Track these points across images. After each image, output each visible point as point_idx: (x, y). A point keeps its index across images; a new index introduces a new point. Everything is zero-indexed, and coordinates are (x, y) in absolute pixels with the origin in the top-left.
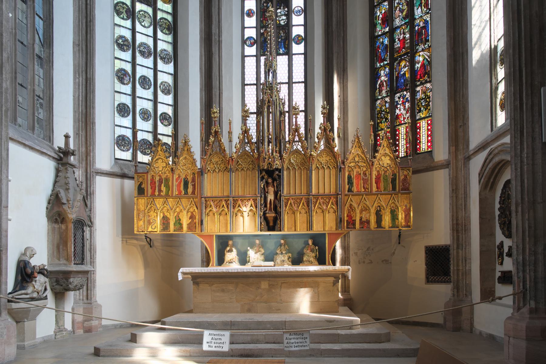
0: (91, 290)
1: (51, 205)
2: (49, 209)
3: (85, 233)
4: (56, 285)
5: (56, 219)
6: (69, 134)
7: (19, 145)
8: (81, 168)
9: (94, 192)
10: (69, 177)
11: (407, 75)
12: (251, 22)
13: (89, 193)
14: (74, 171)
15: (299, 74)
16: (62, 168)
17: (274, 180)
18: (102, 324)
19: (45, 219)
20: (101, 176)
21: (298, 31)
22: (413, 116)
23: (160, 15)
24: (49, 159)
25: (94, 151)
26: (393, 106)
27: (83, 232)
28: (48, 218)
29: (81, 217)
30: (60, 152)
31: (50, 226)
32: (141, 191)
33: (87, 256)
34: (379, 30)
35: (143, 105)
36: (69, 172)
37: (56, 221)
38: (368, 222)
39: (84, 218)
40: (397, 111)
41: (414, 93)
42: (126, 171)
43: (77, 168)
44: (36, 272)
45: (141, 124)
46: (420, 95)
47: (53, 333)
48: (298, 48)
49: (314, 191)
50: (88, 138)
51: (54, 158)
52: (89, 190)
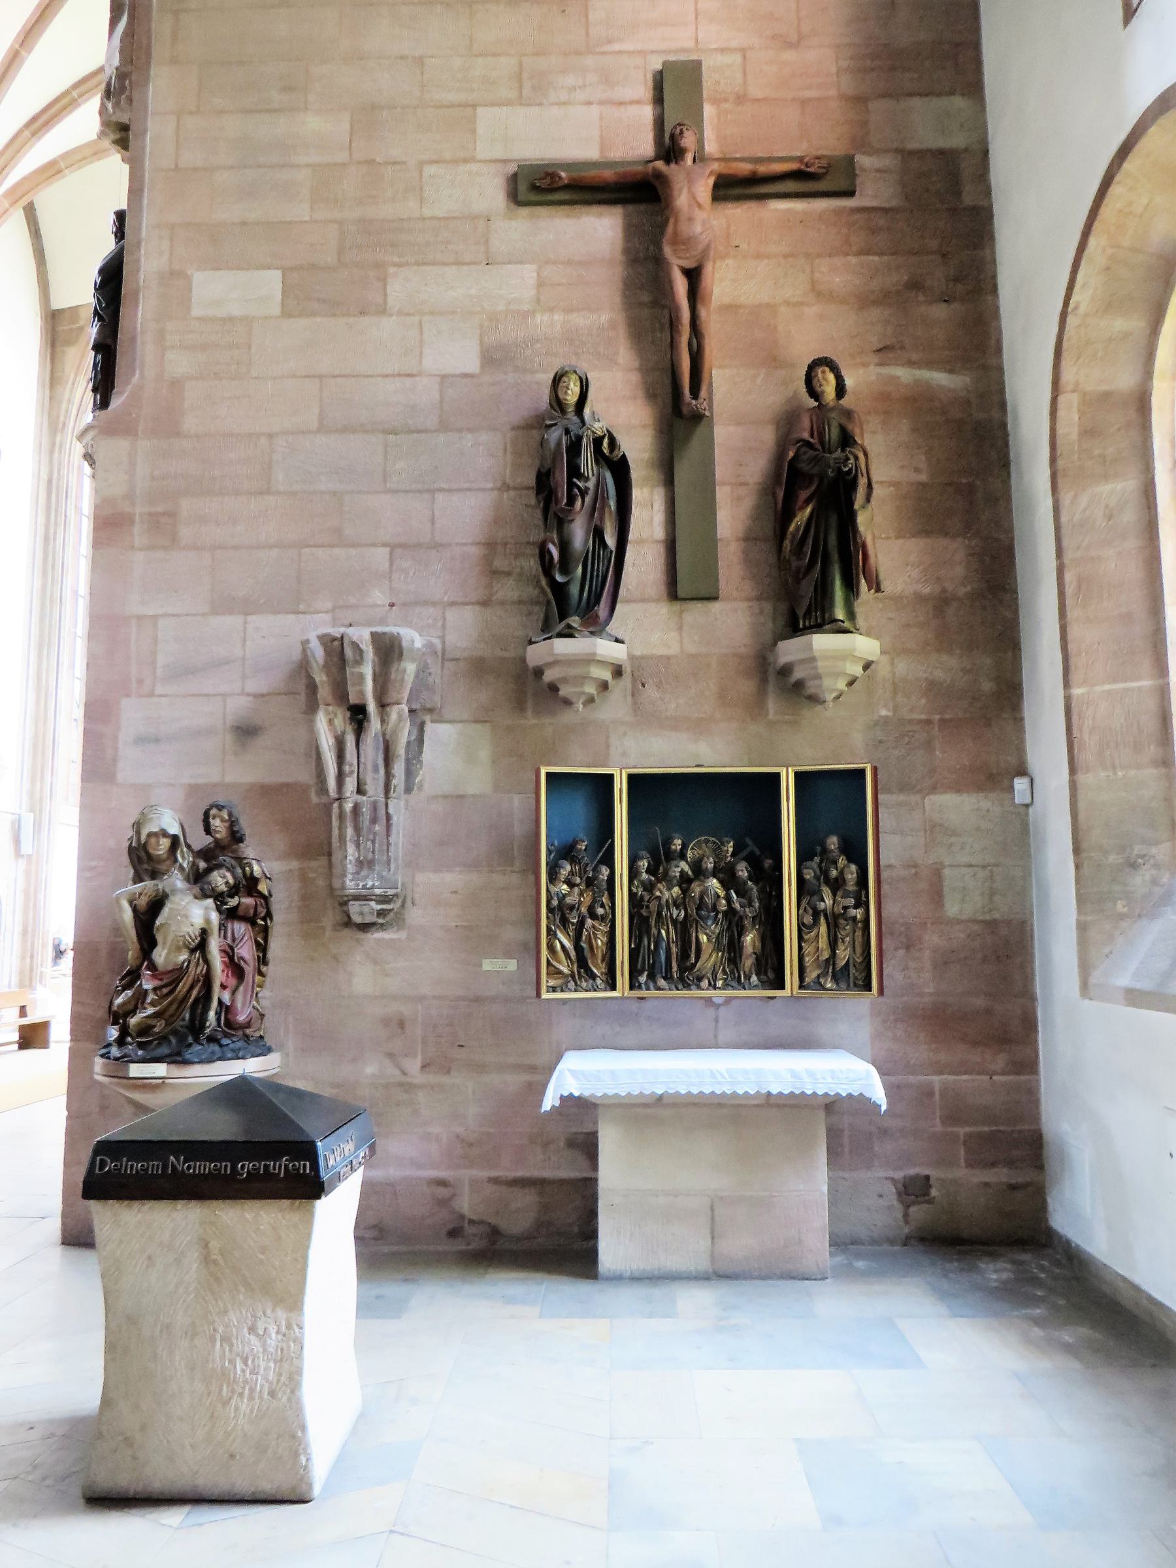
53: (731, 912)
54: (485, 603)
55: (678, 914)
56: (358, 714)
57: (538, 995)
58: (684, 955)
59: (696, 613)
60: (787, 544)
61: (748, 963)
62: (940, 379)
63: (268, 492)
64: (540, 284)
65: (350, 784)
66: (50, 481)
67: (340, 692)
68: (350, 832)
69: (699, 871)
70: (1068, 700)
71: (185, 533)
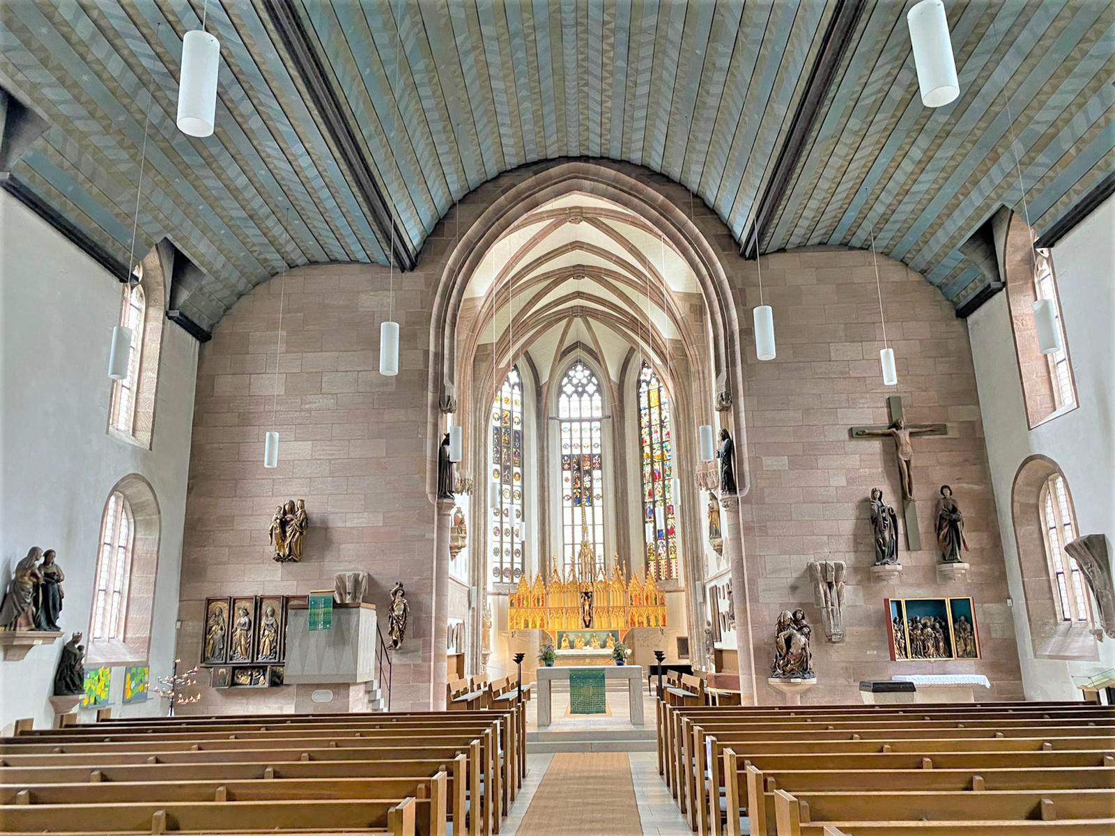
11: (664, 531)
12: (568, 485)
15: (599, 520)
17: (589, 597)
21: (597, 491)
22: (668, 555)
23: (515, 489)
26: (657, 547)
32: (512, 604)
34: (647, 499)
35: (507, 546)
38: (642, 623)
40: (659, 552)
41: (667, 543)
42: (500, 591)
45: (507, 559)
46: (671, 545)
48: (598, 503)
49: (611, 605)
53: (935, 637)
54: (856, 552)
55: (922, 638)
56: (830, 585)
57: (893, 658)
58: (924, 648)
59: (914, 554)
60: (941, 537)
61: (942, 651)
62: (976, 487)
63: (791, 520)
64: (861, 461)
65: (829, 603)
66: (475, 426)
67: (825, 578)
68: (831, 617)
69: (925, 626)
70: (1023, 582)
71: (770, 532)
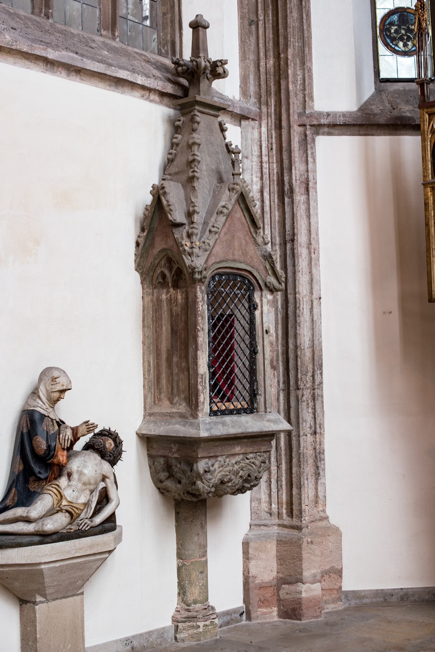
0: (300, 488)
1: (145, 234)
2: (141, 247)
3: (257, 313)
4: (168, 478)
5: (164, 276)
6: (205, 18)
7: (27, 63)
8: (264, 117)
9: (311, 184)
10: (198, 141)
13: (287, 187)
14: (221, 125)
16: (182, 119)
18: (343, 589)
19: (136, 277)
20: (329, 134)
24: (148, 99)
25: (308, 64)
27: (252, 307)
28: (141, 275)
29: (234, 261)
30: (178, 74)
31: (148, 299)
33: (268, 382)
36: (202, 127)
37: (163, 284)
39: (248, 264)
43: (253, 119)
44: (64, 449)
47: (168, 623)
50: (280, 27)
51: (162, 94)
52: (286, 178)
